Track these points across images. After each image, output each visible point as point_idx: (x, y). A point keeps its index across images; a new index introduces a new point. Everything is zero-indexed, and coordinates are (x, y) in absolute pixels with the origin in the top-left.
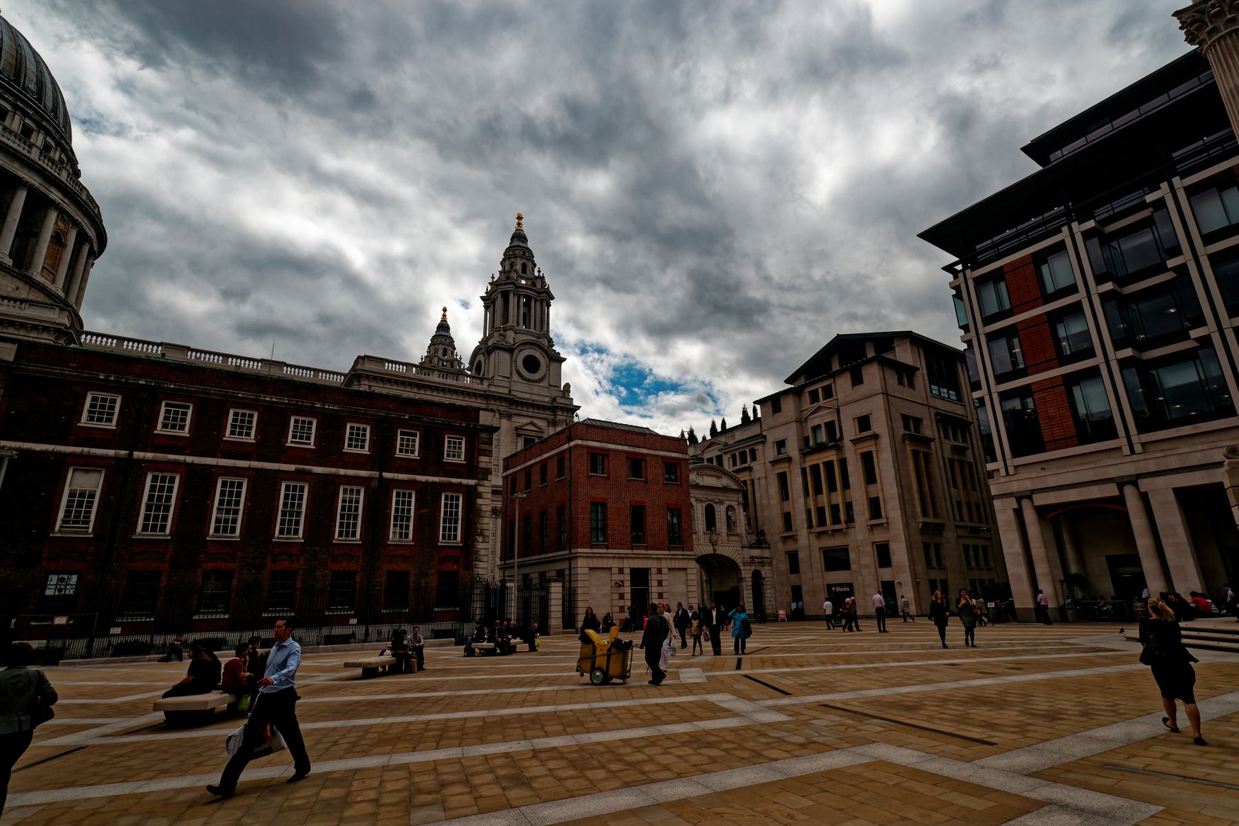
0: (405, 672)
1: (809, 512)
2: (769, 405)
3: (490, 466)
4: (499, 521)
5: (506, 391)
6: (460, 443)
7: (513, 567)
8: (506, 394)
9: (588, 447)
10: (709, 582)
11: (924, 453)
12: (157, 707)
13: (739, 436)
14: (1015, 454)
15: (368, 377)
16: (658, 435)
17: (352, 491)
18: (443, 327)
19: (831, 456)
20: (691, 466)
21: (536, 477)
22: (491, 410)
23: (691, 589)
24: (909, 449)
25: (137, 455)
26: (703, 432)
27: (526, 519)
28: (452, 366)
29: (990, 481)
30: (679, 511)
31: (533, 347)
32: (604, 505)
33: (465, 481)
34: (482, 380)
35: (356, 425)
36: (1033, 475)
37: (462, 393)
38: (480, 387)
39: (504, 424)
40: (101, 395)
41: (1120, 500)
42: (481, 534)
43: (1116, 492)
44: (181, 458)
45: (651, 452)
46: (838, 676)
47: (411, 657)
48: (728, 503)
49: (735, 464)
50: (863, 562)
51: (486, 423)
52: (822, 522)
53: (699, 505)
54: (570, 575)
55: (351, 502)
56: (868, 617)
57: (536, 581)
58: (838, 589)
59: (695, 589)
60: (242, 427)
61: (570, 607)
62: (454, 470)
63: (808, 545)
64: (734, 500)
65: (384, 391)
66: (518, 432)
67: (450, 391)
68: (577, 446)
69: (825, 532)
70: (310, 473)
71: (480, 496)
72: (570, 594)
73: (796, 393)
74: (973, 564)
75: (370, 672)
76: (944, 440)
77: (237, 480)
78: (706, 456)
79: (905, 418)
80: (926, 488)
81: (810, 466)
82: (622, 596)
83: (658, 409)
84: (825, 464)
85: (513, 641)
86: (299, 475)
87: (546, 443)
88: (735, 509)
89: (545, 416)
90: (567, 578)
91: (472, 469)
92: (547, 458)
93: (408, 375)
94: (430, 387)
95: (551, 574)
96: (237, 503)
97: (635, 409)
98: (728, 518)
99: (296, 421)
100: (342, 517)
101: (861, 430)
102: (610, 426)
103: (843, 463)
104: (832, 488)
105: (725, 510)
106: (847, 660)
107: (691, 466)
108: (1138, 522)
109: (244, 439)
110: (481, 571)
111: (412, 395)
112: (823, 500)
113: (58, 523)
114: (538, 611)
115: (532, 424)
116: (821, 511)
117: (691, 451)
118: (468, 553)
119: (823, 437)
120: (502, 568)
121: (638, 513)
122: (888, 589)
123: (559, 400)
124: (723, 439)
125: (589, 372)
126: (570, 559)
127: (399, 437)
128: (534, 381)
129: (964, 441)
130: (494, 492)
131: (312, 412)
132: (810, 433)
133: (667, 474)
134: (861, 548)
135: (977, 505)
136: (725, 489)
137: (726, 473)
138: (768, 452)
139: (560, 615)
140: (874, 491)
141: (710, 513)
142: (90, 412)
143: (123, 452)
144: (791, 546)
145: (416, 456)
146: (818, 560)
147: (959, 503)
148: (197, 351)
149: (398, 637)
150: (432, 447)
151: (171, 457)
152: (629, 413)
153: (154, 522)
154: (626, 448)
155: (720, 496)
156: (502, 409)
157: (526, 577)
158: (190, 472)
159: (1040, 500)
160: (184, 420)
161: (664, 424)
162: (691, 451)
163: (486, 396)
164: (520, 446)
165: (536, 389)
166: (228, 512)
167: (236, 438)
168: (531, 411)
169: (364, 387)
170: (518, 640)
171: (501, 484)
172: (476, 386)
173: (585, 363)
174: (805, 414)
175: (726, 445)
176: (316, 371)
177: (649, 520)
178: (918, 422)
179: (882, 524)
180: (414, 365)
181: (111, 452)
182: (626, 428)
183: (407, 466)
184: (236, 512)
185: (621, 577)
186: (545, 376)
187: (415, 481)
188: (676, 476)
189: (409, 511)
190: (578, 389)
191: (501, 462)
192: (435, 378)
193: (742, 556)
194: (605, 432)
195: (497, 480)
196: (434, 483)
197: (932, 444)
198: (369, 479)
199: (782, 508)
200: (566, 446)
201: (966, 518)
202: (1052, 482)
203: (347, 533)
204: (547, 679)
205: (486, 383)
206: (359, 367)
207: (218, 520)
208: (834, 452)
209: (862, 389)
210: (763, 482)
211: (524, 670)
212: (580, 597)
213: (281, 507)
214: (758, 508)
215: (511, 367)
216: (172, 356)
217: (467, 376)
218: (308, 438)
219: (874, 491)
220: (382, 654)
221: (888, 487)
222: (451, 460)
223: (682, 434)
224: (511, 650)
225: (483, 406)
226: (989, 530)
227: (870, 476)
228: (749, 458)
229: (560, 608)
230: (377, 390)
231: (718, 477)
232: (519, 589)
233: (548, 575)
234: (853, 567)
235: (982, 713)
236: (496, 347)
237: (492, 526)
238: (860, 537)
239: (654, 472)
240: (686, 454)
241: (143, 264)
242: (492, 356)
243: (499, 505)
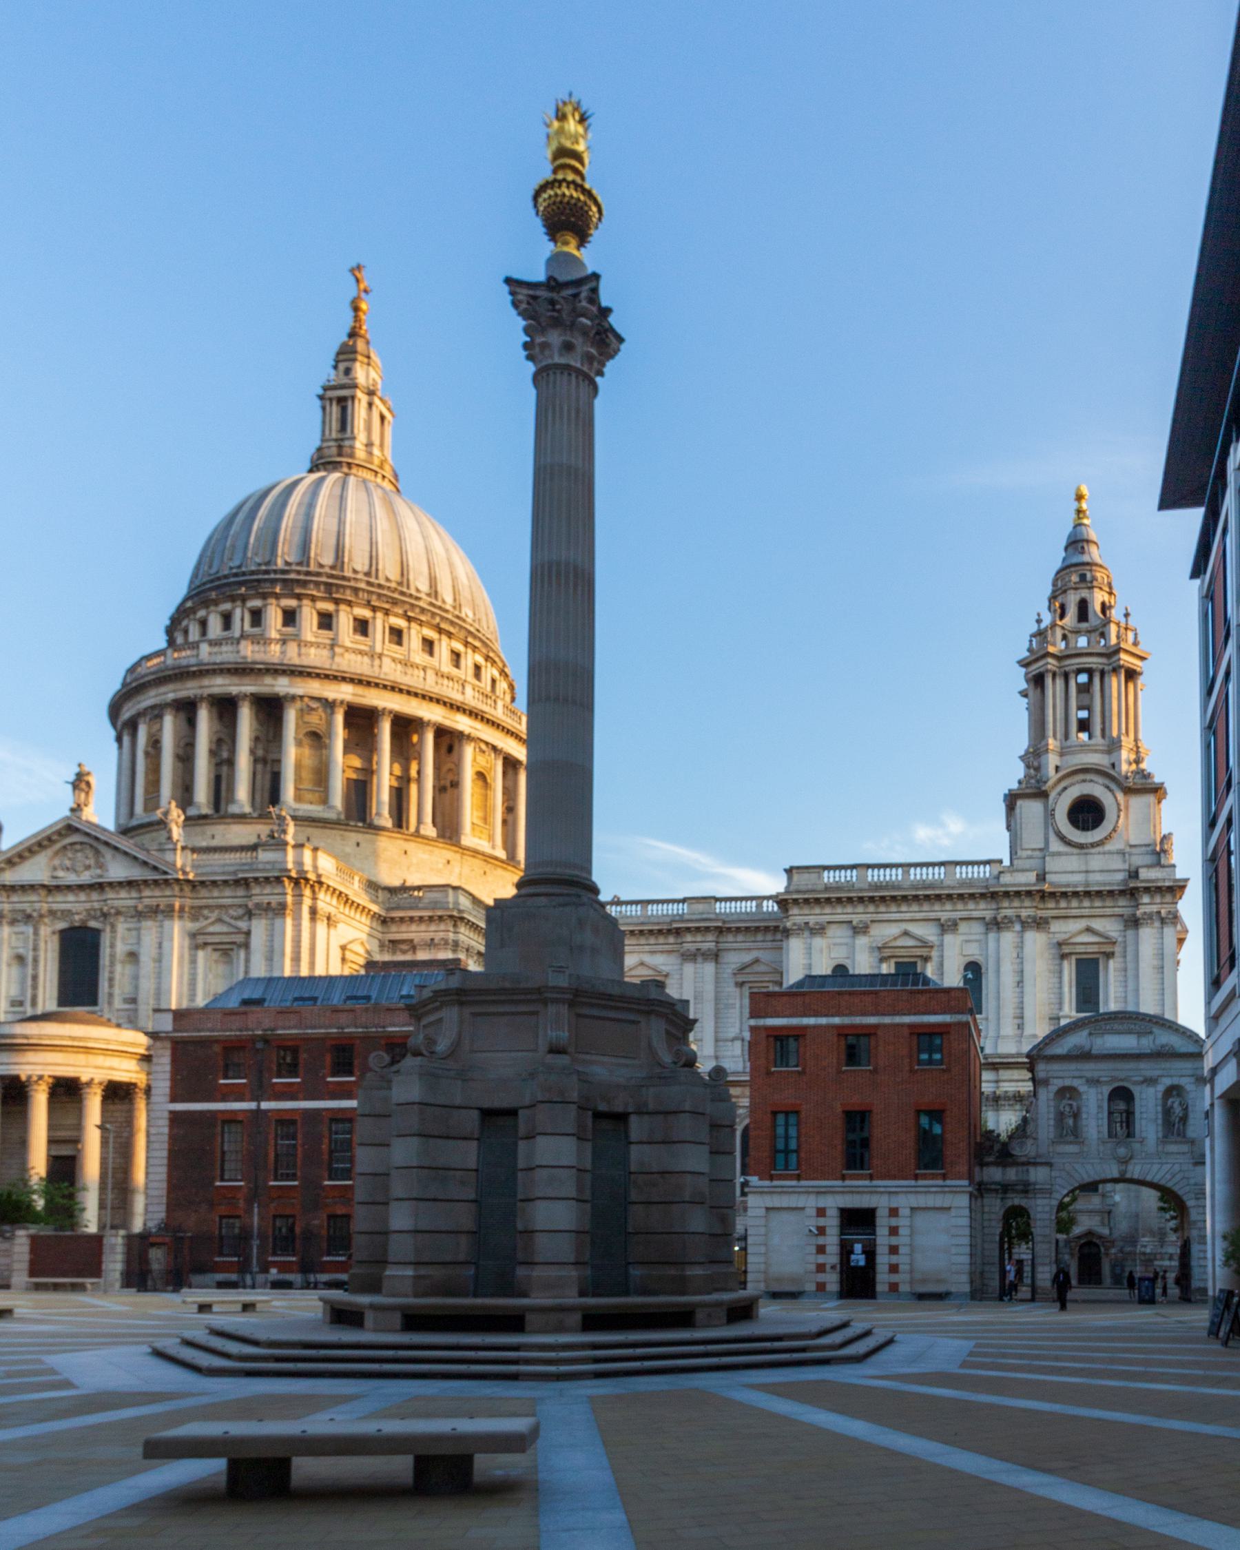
5: (1031, 877)
8: (1034, 885)
31: (1088, 777)
45: (887, 1020)
105: (1160, 1095)
128: (1093, 845)
154: (836, 1020)
156: (1024, 913)
165: (1096, 861)
193: (1192, 1181)
194: (799, 1000)
215: (1046, 828)
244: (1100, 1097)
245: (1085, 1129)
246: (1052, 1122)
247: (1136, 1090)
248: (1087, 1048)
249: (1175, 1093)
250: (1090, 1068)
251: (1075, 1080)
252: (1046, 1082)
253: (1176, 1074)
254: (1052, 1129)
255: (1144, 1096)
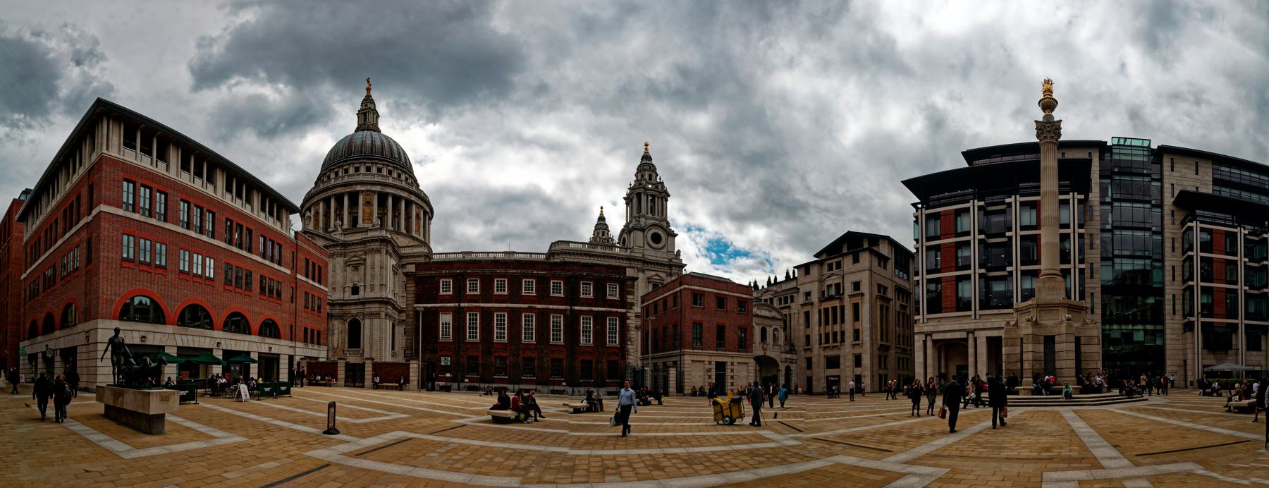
0: (594, 412)
1: (820, 335)
2: (803, 270)
3: (634, 301)
4: (639, 333)
6: (616, 288)
7: (648, 359)
9: (691, 290)
10: (760, 371)
11: (886, 307)
12: (489, 413)
13: (784, 287)
14: (929, 313)
15: (558, 254)
16: (735, 283)
17: (557, 317)
18: (602, 218)
19: (836, 303)
20: (754, 303)
21: (660, 307)
22: (633, 268)
23: (749, 374)
24: (879, 303)
25: (462, 305)
26: (762, 283)
27: (655, 331)
28: (608, 241)
29: (915, 325)
30: (746, 329)
32: (701, 324)
33: (619, 310)
34: (626, 249)
35: (555, 281)
36: (934, 324)
37: (615, 258)
38: (625, 254)
39: (641, 275)
40: (445, 280)
41: (966, 340)
42: (630, 340)
43: (966, 336)
44: (478, 305)
46: (825, 424)
47: (596, 404)
48: (774, 327)
49: (780, 304)
50: (847, 364)
51: (631, 275)
52: (827, 341)
53: (757, 327)
54: (680, 364)
55: (557, 322)
56: (846, 393)
57: (661, 367)
58: (832, 379)
59: (752, 374)
60: (501, 287)
61: (680, 382)
62: (613, 304)
63: (819, 354)
64: (778, 325)
65: (571, 260)
66: (649, 280)
67: (608, 257)
68: (685, 288)
69: (829, 347)
70: (535, 308)
71: (628, 318)
72: (680, 375)
73: (820, 263)
74: (901, 367)
75: (577, 411)
76: (897, 301)
77: (502, 313)
78: (764, 298)
79: (879, 286)
80: (884, 326)
81: (824, 309)
82: (710, 377)
83: (735, 267)
84: (832, 308)
85: (649, 399)
86: (530, 310)
87: (666, 287)
89: (665, 270)
90: (679, 366)
91: (623, 303)
92: (666, 296)
93: (584, 249)
94: (596, 256)
95: (670, 363)
96: (504, 325)
97: (721, 267)
98: (774, 335)
99: (525, 282)
100: (553, 331)
101: (855, 290)
102: (705, 276)
103: (843, 308)
104: (835, 322)
106: (831, 416)
107: (754, 303)
108: (971, 350)
109: (503, 293)
110: (630, 361)
111: (586, 261)
112: (829, 329)
113: (441, 336)
114: (662, 384)
115: (657, 275)
116: (827, 335)
117: (755, 294)
118: (623, 351)
119: (833, 292)
120: (642, 359)
121: (721, 330)
122: (858, 379)
123: (673, 260)
124: (774, 288)
125: (693, 243)
126: (681, 355)
127: (582, 286)
128: (658, 249)
129: (907, 302)
130: (636, 316)
131: (532, 276)
132: (826, 289)
133: (739, 307)
134: (847, 357)
135: (908, 337)
136: (773, 318)
137: (775, 309)
138: (800, 299)
139: (675, 386)
140: (858, 325)
141: (764, 331)
142: (443, 288)
143: (457, 304)
144: (808, 354)
145: (591, 296)
146: (823, 362)
147: (899, 335)
148: (476, 253)
149: (589, 394)
150: (600, 290)
151: (475, 304)
152: (717, 269)
153: (473, 336)
155: (771, 322)
157: (655, 365)
158: (483, 310)
159: (936, 337)
160: (477, 287)
161: (739, 277)
162: (755, 294)
163: (629, 259)
164: (650, 289)
165: (659, 254)
166: (501, 329)
167: (500, 293)
168: (656, 268)
169: (557, 259)
170: (652, 398)
171: (640, 311)
172: (623, 253)
173: (690, 237)
174: (824, 277)
175: (776, 292)
176: (531, 254)
177: (727, 334)
178: (885, 289)
179: (859, 344)
180: (586, 243)
181: (452, 305)
182: (716, 279)
183: (587, 302)
184: (504, 329)
185: (710, 366)
186: (664, 246)
187: (592, 311)
188: (745, 309)
189: (590, 327)
190: (686, 254)
191: (640, 299)
192: (599, 250)
195: (637, 309)
196: (601, 311)
197: (891, 302)
198: (565, 310)
199: (805, 332)
200: (678, 289)
201: (901, 343)
202: (942, 328)
203: (557, 339)
204: (669, 419)
205: (629, 251)
206: (553, 249)
207: (497, 333)
208: (838, 301)
209: (858, 266)
210: (796, 315)
211: (657, 414)
212: (686, 377)
213: (523, 326)
214: (792, 331)
216: (468, 257)
217: (618, 247)
218: (532, 290)
219: (858, 325)
220: (582, 402)
221: (865, 324)
222: (611, 298)
223: (750, 284)
224: (649, 403)
225: (628, 265)
226: (911, 350)
227: (856, 317)
228: (789, 301)
229: (675, 382)
230: (567, 260)
231: (771, 311)
232: (652, 371)
233: (668, 363)
234: (842, 367)
235: (890, 438)
236: (634, 229)
237: (635, 336)
238: (847, 350)
239: (731, 306)
240: (752, 295)
241: (450, 217)
242: (632, 234)
243: (639, 324)
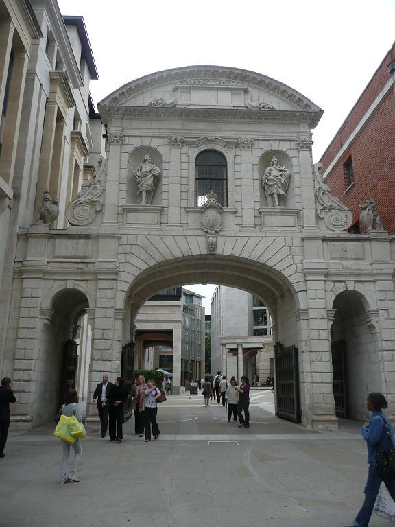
88: (289, 160)
105: (256, 161)
244: (184, 158)
245: (164, 196)
246: (124, 187)
247: (229, 154)
248: (169, 101)
249: (275, 159)
250: (176, 128)
251: (154, 139)
252: (120, 141)
253: (277, 137)
254: (124, 195)
255: (238, 159)
